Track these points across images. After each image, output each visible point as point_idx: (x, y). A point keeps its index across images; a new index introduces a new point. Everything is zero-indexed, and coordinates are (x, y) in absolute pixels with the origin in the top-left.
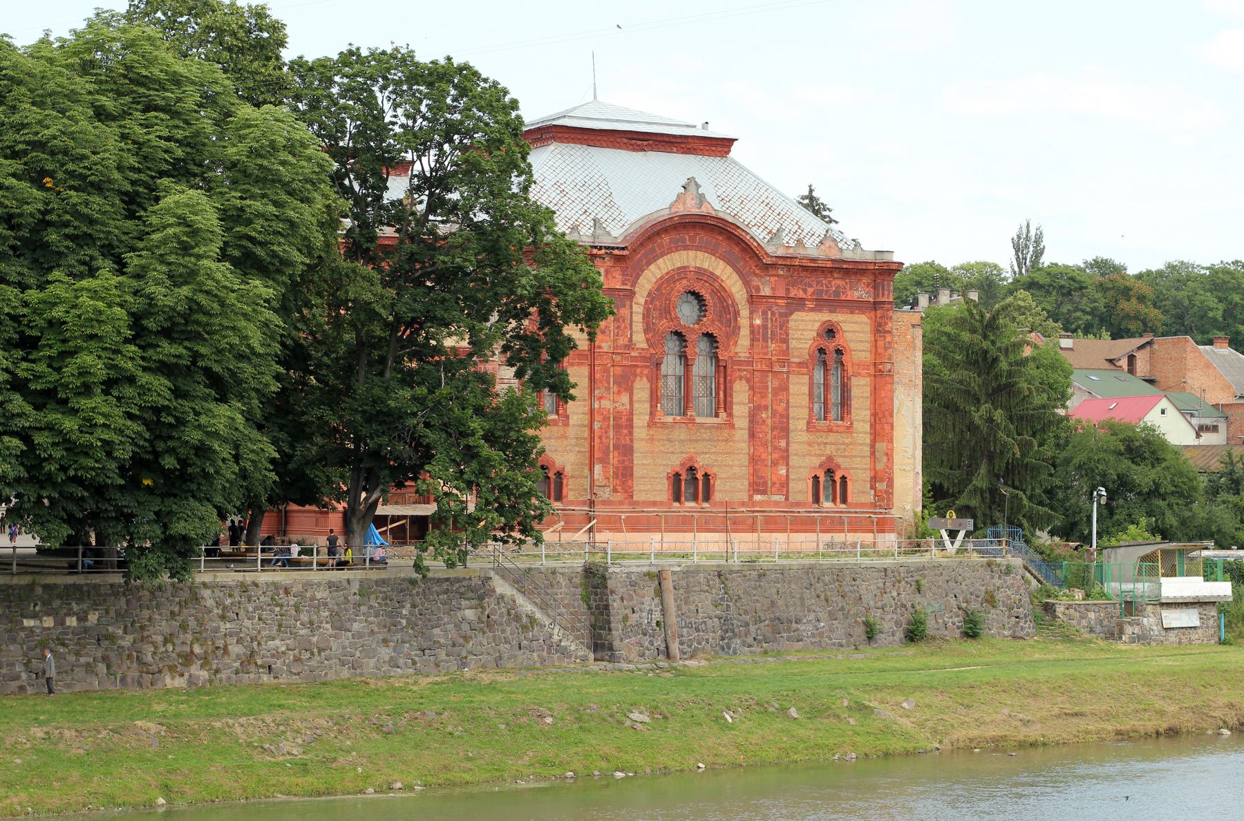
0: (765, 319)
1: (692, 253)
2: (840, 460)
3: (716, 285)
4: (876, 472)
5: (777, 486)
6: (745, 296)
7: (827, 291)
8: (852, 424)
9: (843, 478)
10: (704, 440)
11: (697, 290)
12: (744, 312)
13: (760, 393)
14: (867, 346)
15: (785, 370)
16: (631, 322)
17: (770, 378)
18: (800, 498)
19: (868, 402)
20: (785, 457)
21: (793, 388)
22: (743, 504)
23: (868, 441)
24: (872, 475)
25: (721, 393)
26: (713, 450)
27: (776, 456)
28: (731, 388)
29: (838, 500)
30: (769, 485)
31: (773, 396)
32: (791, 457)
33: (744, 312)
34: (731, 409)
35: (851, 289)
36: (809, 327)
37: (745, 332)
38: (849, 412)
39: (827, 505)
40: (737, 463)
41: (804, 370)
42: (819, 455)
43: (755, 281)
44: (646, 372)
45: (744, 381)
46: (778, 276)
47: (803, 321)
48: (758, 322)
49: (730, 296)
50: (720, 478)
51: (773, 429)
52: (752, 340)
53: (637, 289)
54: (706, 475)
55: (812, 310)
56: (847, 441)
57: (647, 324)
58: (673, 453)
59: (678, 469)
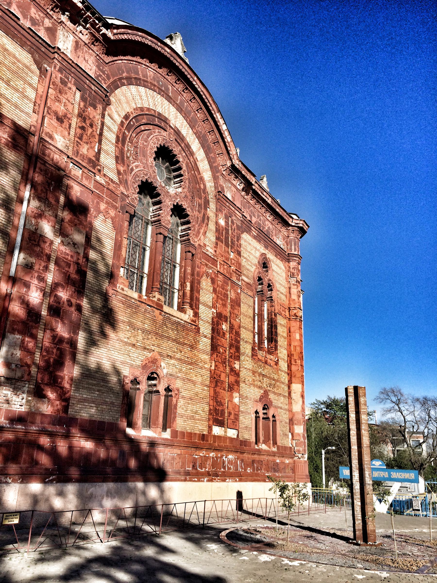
0: (227, 223)
1: (173, 110)
2: (271, 396)
3: (192, 160)
4: (293, 414)
5: (232, 417)
6: (213, 189)
7: (264, 228)
8: (278, 360)
9: (274, 416)
10: (169, 338)
11: (176, 150)
12: (212, 206)
13: (222, 300)
14: (283, 290)
15: (240, 283)
16: (101, 134)
17: (229, 288)
18: (246, 436)
19: (286, 343)
20: (238, 383)
21: (244, 308)
22: (203, 437)
23: (287, 382)
24: (291, 417)
25: (188, 284)
26: (178, 356)
27: (232, 379)
28: (199, 283)
29: (272, 442)
30: (226, 415)
31: (232, 307)
32: (242, 385)
33: (212, 206)
34: (198, 309)
35: (276, 235)
36: (253, 252)
37: (212, 226)
38: (276, 349)
39: (264, 447)
40: (200, 379)
41: (250, 293)
42: (260, 387)
43: (221, 181)
44: (112, 213)
45: (209, 280)
46: (237, 189)
47: (250, 244)
48: (222, 222)
49: (202, 179)
50: (183, 397)
51: (231, 346)
52: (218, 238)
53: (112, 99)
54: (168, 389)
55: (255, 237)
56: (276, 377)
57: (122, 152)
58: (134, 345)
59: (137, 373)
